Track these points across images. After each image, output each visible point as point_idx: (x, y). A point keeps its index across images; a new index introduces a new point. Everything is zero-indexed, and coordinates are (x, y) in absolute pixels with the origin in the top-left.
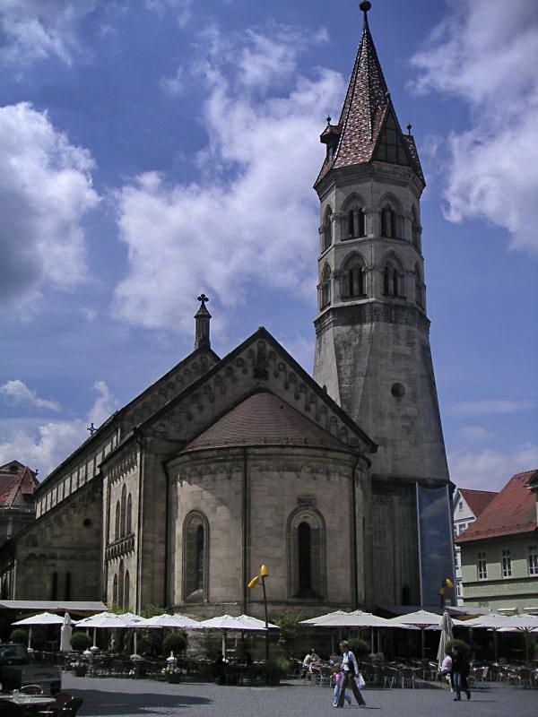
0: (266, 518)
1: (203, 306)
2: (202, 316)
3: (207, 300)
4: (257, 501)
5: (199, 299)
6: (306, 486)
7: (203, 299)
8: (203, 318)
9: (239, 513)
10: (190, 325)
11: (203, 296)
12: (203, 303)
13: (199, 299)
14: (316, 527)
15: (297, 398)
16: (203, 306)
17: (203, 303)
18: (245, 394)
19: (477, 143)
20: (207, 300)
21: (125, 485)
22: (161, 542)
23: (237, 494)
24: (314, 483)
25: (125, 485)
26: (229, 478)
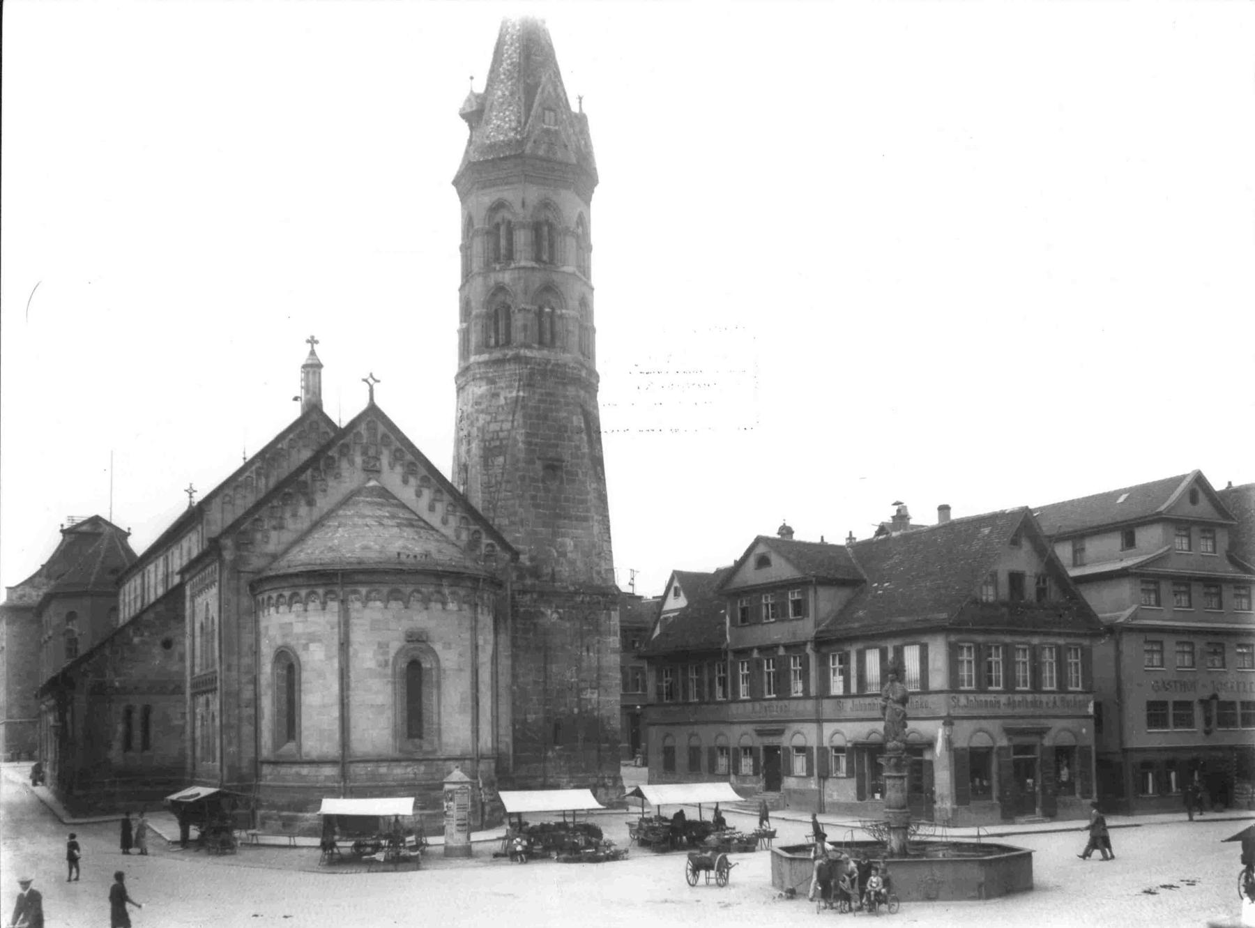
0: (366, 658)
1: (313, 353)
2: (311, 366)
3: (317, 342)
4: (357, 636)
5: (308, 341)
6: (420, 619)
7: (312, 341)
8: (313, 368)
9: (335, 649)
10: (295, 385)
11: (313, 337)
12: (312, 347)
13: (308, 341)
14: (428, 666)
15: (419, 494)
16: (313, 353)
17: (312, 347)
18: (352, 491)
19: (167, 644)
20: (317, 342)
21: (207, 605)
22: (249, 682)
23: (332, 628)
24: (425, 613)
25: (207, 605)
26: (324, 609)
